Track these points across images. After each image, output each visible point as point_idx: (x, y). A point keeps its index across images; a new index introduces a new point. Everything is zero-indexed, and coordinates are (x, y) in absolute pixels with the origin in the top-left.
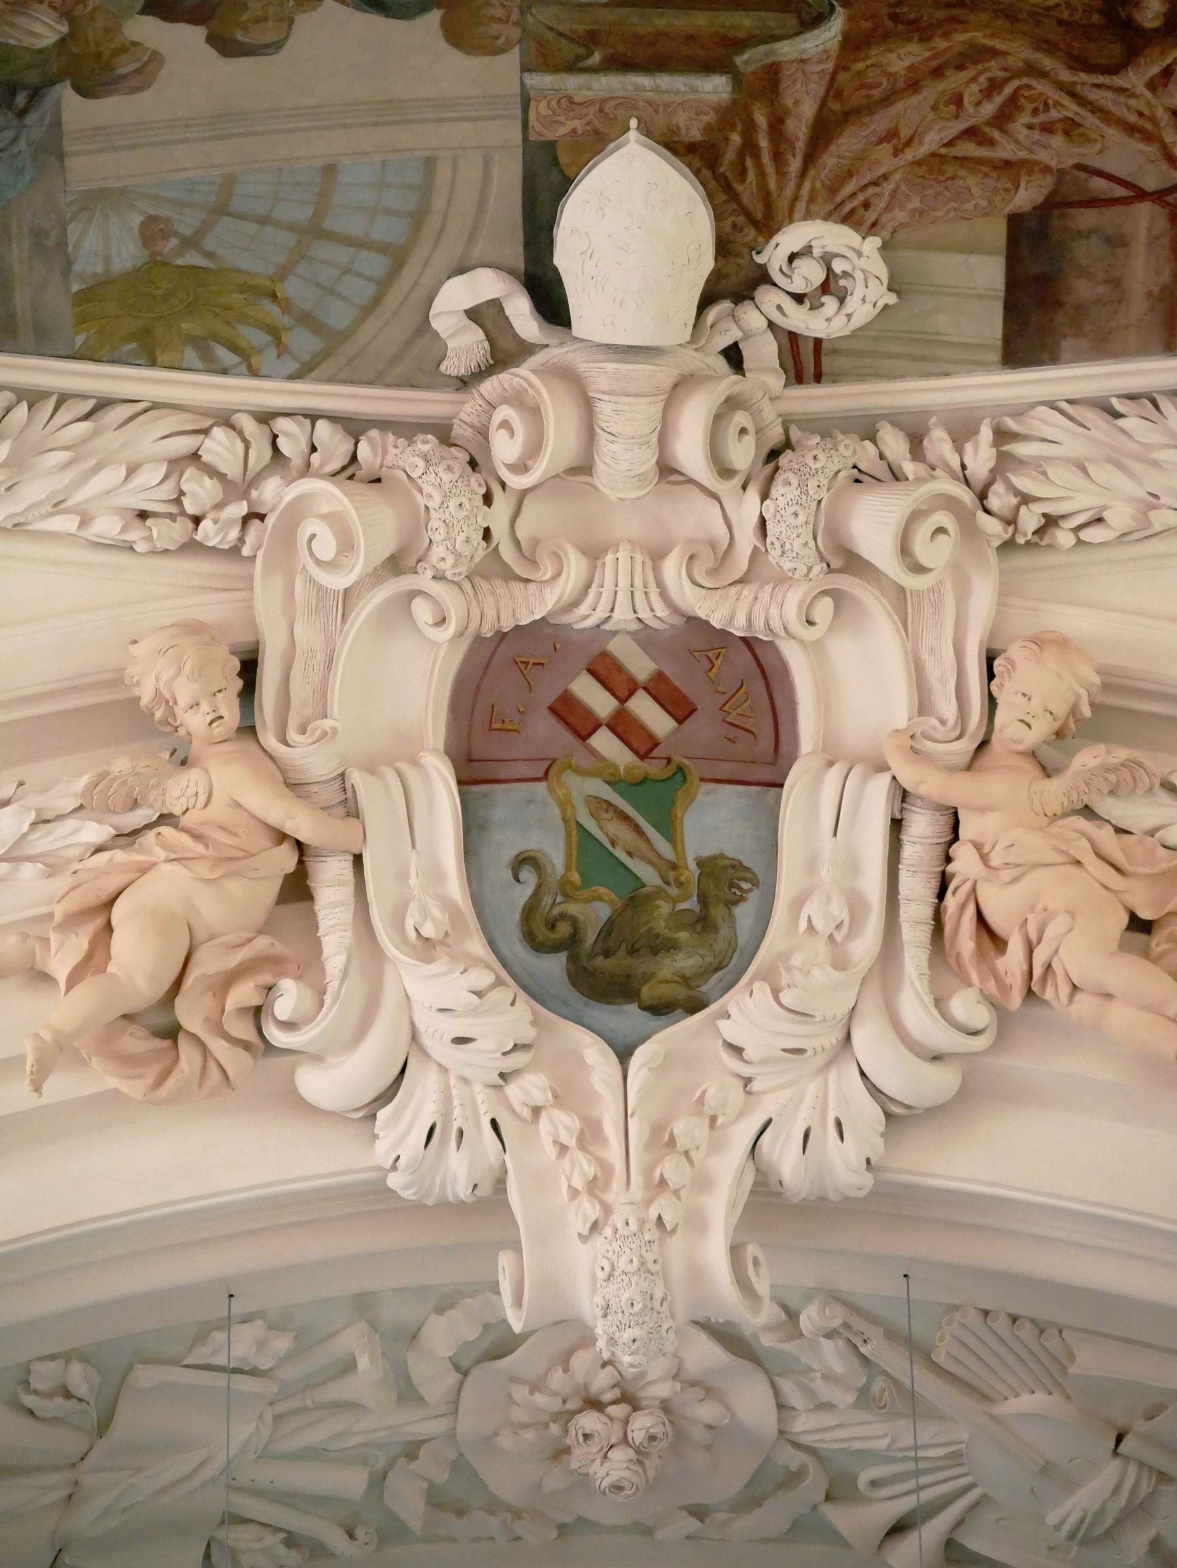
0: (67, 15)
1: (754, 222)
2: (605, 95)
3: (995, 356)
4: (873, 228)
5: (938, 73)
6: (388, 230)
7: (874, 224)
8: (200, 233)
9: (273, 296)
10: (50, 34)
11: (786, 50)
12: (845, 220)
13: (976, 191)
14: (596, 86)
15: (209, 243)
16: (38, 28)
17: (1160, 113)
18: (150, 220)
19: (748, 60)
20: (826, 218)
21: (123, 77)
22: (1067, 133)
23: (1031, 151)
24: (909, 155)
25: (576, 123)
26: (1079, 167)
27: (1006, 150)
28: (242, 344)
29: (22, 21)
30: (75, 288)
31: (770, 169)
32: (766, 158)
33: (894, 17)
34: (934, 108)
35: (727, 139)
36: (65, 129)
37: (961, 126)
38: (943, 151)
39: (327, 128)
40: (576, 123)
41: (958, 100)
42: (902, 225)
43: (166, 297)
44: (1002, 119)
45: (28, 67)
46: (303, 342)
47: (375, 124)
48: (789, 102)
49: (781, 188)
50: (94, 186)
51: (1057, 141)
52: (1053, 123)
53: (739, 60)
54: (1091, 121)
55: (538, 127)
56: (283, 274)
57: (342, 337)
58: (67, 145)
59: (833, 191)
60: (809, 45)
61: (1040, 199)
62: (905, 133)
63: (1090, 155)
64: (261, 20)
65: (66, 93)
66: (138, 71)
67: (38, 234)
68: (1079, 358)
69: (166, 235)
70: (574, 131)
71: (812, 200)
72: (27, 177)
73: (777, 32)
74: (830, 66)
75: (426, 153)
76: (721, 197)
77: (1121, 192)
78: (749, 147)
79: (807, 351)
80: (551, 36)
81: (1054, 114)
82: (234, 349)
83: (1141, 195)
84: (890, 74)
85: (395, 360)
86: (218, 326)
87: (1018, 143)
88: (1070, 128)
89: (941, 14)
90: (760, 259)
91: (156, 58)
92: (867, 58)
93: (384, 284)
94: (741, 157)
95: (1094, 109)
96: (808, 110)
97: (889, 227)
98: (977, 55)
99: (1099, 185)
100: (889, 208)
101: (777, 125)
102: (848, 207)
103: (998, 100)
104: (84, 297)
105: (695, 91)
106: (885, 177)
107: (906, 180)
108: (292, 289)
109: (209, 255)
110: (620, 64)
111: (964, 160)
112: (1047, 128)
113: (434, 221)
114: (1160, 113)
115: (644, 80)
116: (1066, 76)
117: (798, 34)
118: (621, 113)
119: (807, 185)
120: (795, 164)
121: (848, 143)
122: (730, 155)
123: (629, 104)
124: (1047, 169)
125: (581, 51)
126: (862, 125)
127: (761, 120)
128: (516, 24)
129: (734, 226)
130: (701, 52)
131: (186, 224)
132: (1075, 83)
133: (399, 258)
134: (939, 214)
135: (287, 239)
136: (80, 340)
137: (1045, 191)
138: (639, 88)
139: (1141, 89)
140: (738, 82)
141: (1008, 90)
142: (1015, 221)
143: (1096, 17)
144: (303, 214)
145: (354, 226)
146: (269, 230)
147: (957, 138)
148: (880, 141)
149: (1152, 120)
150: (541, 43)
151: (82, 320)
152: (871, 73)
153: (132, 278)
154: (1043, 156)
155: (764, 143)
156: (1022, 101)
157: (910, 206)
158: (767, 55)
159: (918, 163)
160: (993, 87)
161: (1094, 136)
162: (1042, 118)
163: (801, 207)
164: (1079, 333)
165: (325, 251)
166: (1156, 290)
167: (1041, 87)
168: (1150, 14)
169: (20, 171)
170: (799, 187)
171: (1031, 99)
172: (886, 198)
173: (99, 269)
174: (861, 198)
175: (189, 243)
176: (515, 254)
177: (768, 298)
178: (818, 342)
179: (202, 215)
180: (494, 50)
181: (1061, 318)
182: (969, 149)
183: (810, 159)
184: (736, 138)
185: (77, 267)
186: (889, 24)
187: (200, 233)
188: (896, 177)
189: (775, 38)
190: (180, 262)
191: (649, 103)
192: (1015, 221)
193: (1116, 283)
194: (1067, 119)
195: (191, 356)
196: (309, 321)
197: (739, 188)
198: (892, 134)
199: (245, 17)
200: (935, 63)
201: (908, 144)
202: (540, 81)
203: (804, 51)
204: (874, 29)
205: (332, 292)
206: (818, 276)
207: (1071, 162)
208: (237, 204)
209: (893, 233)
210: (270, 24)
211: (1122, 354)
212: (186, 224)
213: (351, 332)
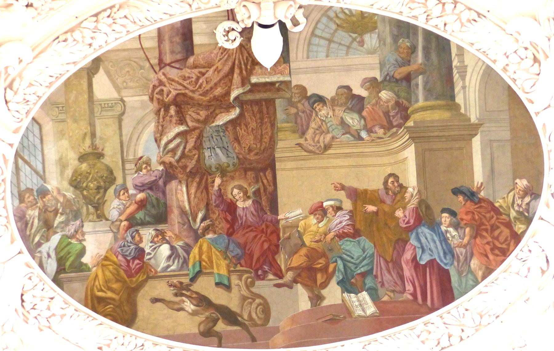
0: (379, 98)
1: (244, 47)
2: (275, 76)
3: (193, 20)
4: (220, 48)
5: (211, 88)
6: (316, 41)
7: (220, 49)
8: (352, 42)
9: (338, 25)
10: (383, 94)
11: (241, 91)
12: (226, 49)
13: (201, 60)
14: (277, 78)
15: (350, 39)
16: (385, 95)
17: (168, 85)
18: (362, 46)
19: (248, 87)
20: (229, 49)
21: (368, 82)
22: (185, 77)
23: (191, 72)
24: (215, 67)
25: (280, 68)
26: (182, 69)
27: (196, 71)
28: (344, 14)
29: (388, 98)
30: (377, 30)
31: (241, 60)
32: (242, 63)
33: (221, 101)
34: (211, 80)
35: (251, 67)
36: (379, 70)
37: (206, 76)
38: (208, 69)
39: (328, 67)
40: (280, 68)
41: (207, 82)
42: (214, 49)
43: (359, 27)
44: (198, 79)
45: (387, 86)
46: (331, 14)
47: (319, 67)
48: (239, 77)
49: (239, 56)
50: (373, 55)
51: (187, 75)
52: (188, 79)
53: (249, 87)
54: (181, 81)
55: (287, 67)
56: (336, 31)
57: (323, 15)
58: (378, 65)
59: (229, 56)
60: (237, 92)
61: (189, 60)
62: (216, 73)
63: (180, 73)
64: (342, 94)
65: (379, 79)
66: (365, 83)
67: (384, 44)
68: (176, 23)
69: (359, 42)
70: (280, 66)
71: (233, 53)
72: (387, 58)
73: (243, 95)
74: (232, 87)
75: (308, 60)
76: (250, 52)
77: (173, 65)
78: (246, 65)
79: (231, 17)
80: (286, 90)
81: (188, 82)
82: (345, 13)
83: (169, 65)
84: (221, 87)
85: (313, 10)
86: (349, 19)
87: (194, 73)
88: (184, 78)
89: (212, 103)
90: (242, 38)
91: (362, 86)
92: (225, 90)
93: (315, 28)
94: (247, 63)
95: (180, 84)
96: (235, 76)
97: (217, 48)
98: (205, 94)
99: (177, 65)
100: (218, 53)
101: (241, 72)
102: (225, 53)
103: (199, 84)
104: (375, 28)
105: (258, 78)
106: (219, 61)
107: (214, 60)
108: (334, 27)
109: (351, 36)
110: (272, 84)
111: (204, 67)
112: (189, 78)
113: (306, 43)
114: (168, 85)
115: (268, 80)
116: (187, 91)
117: (239, 95)
118: (271, 72)
119: (234, 57)
120: (237, 62)
121: (227, 68)
122: (250, 62)
123: (270, 74)
124: (188, 68)
125: (281, 87)
126: (224, 73)
127: (244, 72)
128: (293, 93)
129: (247, 45)
130: (257, 88)
131: (355, 44)
132: (185, 90)
133: (313, 34)
134: (207, 53)
135: (335, 39)
136: (376, 18)
137: (188, 62)
138: (268, 78)
139: (172, 90)
140: (250, 81)
141: (198, 86)
142: (193, 54)
143: (183, 107)
144: (333, 45)
145: (323, 42)
146: (339, 42)
147: (206, 73)
148: (221, 69)
149: (169, 83)
150: (288, 88)
151: (376, 23)
152: (224, 87)
153: (366, 32)
154: (189, 71)
155: (243, 66)
156: (194, 84)
157: (214, 54)
158: (244, 89)
159: (213, 65)
160: (200, 87)
161: (180, 77)
162: (190, 80)
163: (235, 52)
164: (177, 29)
165: (327, 36)
166: (164, 42)
167: (191, 88)
168: (173, 109)
169: (388, 60)
170: (235, 56)
171: (193, 84)
172: (219, 55)
173: (372, 35)
174: (223, 55)
175: (354, 39)
176: (290, 36)
177: (240, 30)
178: (229, 19)
179: (352, 46)
180: (296, 86)
181: (181, 31)
182: (203, 70)
183: (234, 64)
184: (249, 67)
185: (377, 36)
186: (222, 99)
187: (352, 42)
188: (217, 61)
189: (243, 93)
190: (356, 35)
191: (266, 75)
192: (193, 54)
193: (171, 42)
194: (185, 81)
195: (354, 12)
196: (331, 19)
197: (247, 55)
198: (218, 72)
199: (345, 96)
200: (212, 91)
201: (215, 70)
202: (287, 79)
203: (238, 90)
204: (225, 98)
205: (326, 26)
206: (230, 34)
207: (184, 70)
208: (345, 48)
209: (216, 47)
210: (340, 93)
211: (168, 25)
212: (355, 44)
213: (322, 16)
